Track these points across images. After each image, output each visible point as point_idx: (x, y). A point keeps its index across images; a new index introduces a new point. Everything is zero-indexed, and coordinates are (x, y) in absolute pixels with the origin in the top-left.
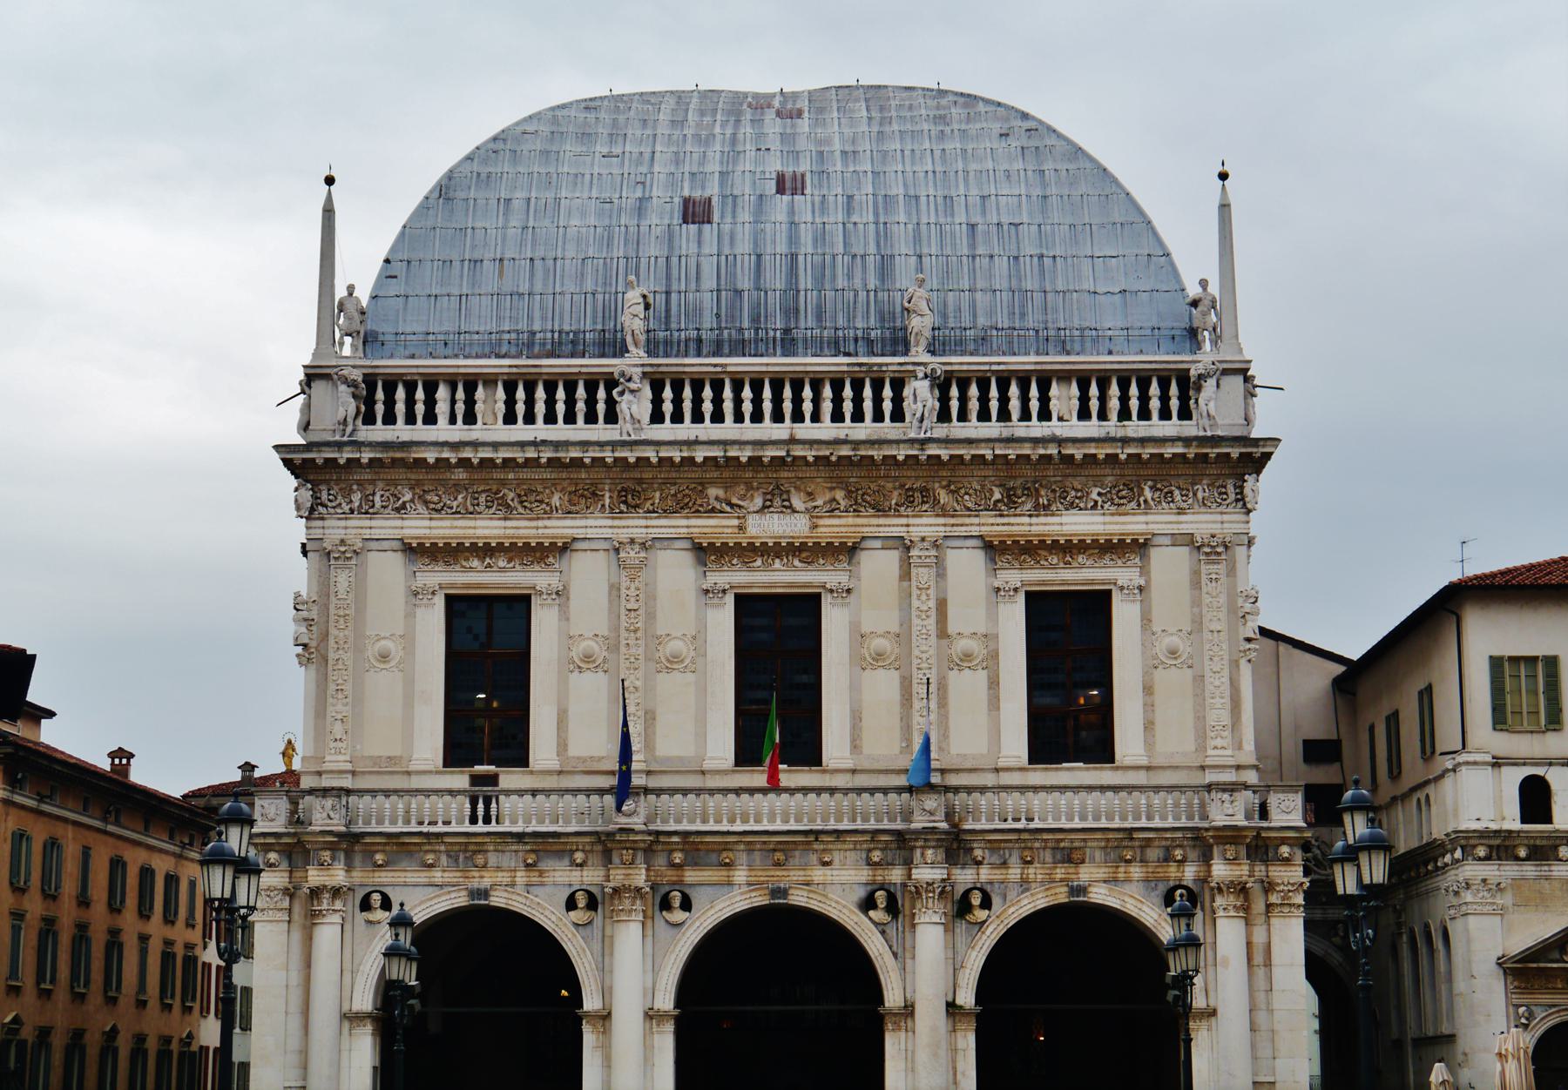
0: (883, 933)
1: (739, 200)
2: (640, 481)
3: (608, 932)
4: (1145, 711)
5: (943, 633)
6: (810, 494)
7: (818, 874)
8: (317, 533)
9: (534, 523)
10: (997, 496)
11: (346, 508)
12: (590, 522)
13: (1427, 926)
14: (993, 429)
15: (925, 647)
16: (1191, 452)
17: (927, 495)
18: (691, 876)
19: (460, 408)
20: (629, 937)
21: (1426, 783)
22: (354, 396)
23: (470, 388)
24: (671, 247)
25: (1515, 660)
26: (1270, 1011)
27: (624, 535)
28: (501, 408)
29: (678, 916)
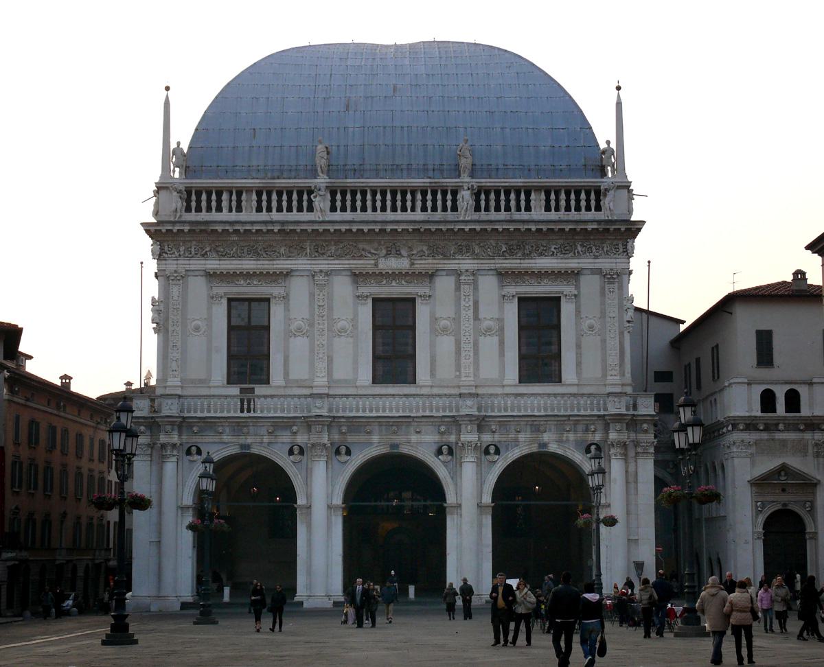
0: (446, 466)
2: (325, 241)
3: (309, 466)
4: (577, 357)
5: (476, 318)
6: (410, 247)
7: (414, 438)
8: (163, 267)
9: (271, 262)
10: (504, 249)
11: (177, 255)
12: (300, 262)
13: (714, 463)
14: (503, 215)
15: (467, 325)
16: (601, 227)
17: (468, 248)
18: (351, 438)
19: (234, 204)
20: (320, 470)
21: (715, 392)
22: (181, 198)
23: (239, 194)
26: (637, 505)
27: (317, 268)
28: (254, 204)
29: (344, 458)
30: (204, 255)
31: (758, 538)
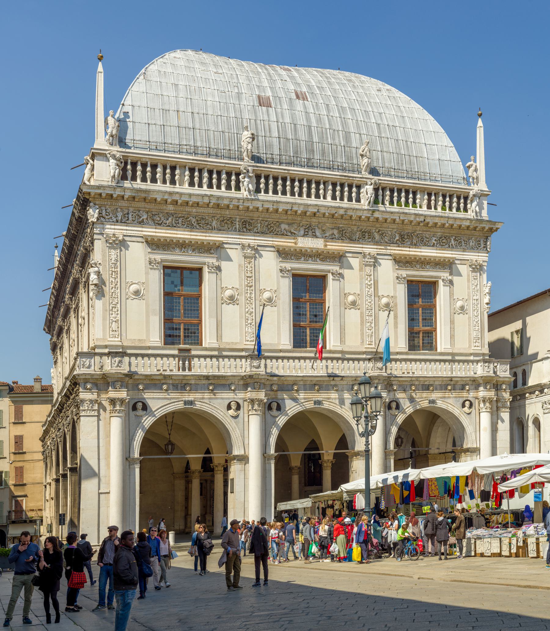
1: (281, 99)
6: (323, 231)
10: (397, 238)
24: (256, 116)
30: (141, 223)
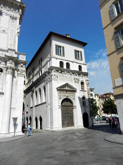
25: (59, 46)
31: (60, 108)
